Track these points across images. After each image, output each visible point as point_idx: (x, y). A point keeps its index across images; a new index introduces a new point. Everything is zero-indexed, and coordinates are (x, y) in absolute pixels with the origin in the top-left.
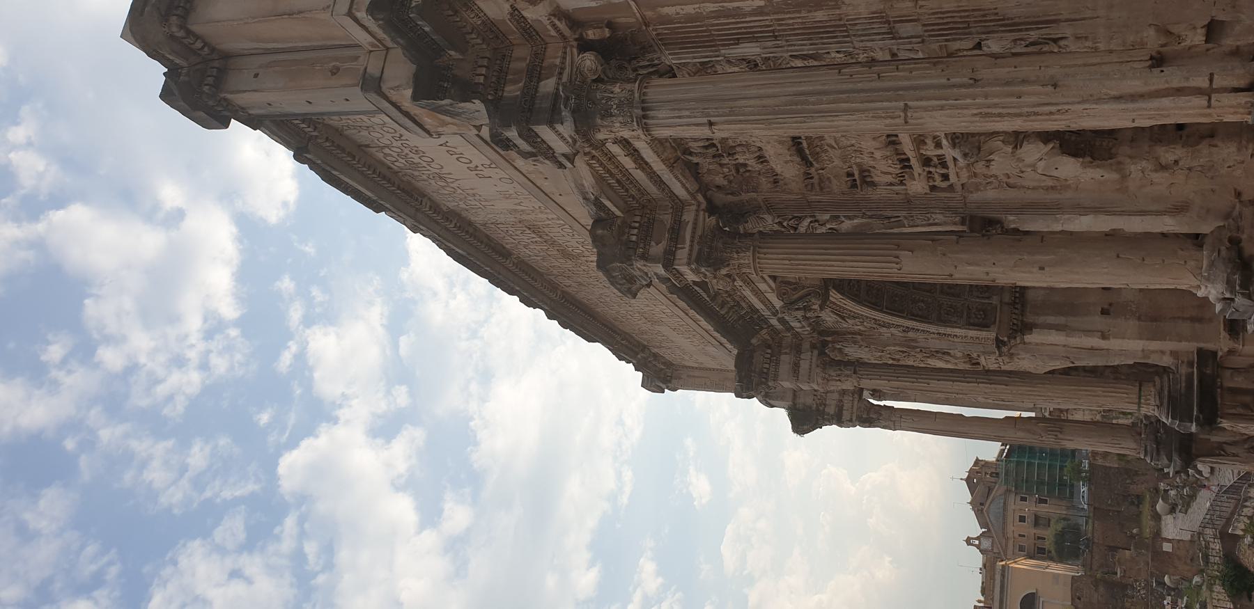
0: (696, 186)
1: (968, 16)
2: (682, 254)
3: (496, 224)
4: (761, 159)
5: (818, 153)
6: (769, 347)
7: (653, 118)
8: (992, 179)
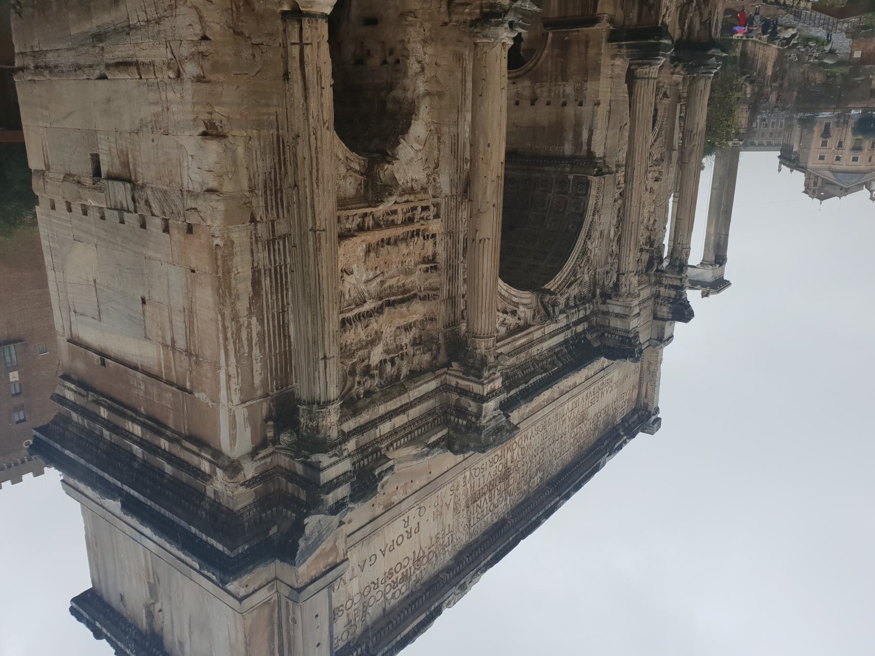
0: (430, 373)
1: (271, 190)
2: (476, 388)
3: (469, 526)
4: (408, 328)
5: (404, 290)
6: (603, 334)
7: (320, 398)
8: (431, 179)
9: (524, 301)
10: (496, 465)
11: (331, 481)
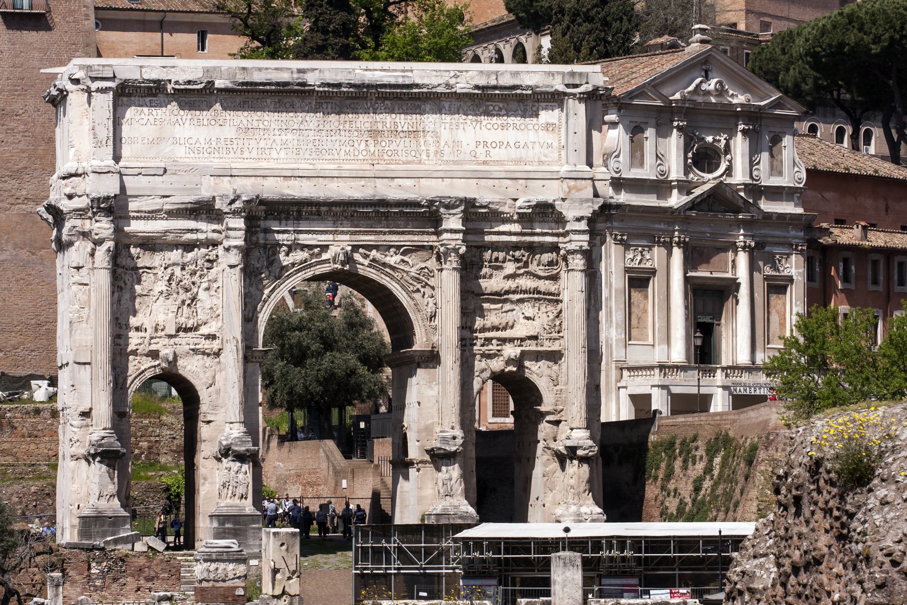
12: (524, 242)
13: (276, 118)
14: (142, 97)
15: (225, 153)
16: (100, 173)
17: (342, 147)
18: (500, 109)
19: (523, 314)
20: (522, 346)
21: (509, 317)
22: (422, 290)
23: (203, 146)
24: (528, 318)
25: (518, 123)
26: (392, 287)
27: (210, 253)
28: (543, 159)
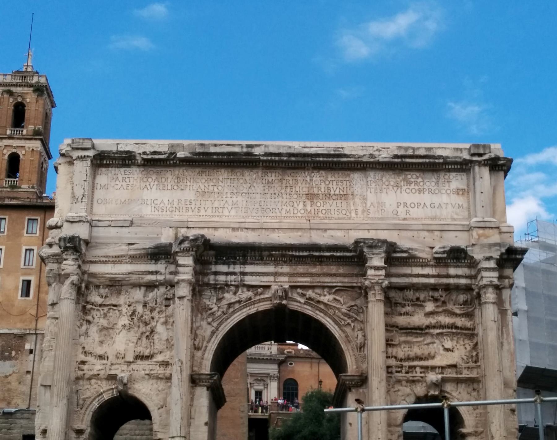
9: (299, 304)
10: (323, 208)
11: (493, 271)
12: (440, 285)
13: (229, 184)
14: (118, 167)
15: (184, 211)
16: (72, 222)
17: (283, 207)
18: (417, 177)
19: (443, 346)
20: (443, 373)
21: (432, 349)
22: (352, 325)
23: (166, 205)
24: (447, 350)
25: (433, 188)
26: (326, 322)
27: (168, 293)
28: (455, 217)
